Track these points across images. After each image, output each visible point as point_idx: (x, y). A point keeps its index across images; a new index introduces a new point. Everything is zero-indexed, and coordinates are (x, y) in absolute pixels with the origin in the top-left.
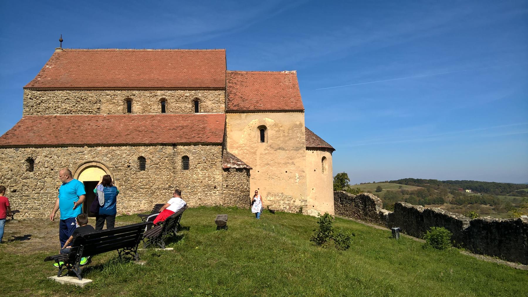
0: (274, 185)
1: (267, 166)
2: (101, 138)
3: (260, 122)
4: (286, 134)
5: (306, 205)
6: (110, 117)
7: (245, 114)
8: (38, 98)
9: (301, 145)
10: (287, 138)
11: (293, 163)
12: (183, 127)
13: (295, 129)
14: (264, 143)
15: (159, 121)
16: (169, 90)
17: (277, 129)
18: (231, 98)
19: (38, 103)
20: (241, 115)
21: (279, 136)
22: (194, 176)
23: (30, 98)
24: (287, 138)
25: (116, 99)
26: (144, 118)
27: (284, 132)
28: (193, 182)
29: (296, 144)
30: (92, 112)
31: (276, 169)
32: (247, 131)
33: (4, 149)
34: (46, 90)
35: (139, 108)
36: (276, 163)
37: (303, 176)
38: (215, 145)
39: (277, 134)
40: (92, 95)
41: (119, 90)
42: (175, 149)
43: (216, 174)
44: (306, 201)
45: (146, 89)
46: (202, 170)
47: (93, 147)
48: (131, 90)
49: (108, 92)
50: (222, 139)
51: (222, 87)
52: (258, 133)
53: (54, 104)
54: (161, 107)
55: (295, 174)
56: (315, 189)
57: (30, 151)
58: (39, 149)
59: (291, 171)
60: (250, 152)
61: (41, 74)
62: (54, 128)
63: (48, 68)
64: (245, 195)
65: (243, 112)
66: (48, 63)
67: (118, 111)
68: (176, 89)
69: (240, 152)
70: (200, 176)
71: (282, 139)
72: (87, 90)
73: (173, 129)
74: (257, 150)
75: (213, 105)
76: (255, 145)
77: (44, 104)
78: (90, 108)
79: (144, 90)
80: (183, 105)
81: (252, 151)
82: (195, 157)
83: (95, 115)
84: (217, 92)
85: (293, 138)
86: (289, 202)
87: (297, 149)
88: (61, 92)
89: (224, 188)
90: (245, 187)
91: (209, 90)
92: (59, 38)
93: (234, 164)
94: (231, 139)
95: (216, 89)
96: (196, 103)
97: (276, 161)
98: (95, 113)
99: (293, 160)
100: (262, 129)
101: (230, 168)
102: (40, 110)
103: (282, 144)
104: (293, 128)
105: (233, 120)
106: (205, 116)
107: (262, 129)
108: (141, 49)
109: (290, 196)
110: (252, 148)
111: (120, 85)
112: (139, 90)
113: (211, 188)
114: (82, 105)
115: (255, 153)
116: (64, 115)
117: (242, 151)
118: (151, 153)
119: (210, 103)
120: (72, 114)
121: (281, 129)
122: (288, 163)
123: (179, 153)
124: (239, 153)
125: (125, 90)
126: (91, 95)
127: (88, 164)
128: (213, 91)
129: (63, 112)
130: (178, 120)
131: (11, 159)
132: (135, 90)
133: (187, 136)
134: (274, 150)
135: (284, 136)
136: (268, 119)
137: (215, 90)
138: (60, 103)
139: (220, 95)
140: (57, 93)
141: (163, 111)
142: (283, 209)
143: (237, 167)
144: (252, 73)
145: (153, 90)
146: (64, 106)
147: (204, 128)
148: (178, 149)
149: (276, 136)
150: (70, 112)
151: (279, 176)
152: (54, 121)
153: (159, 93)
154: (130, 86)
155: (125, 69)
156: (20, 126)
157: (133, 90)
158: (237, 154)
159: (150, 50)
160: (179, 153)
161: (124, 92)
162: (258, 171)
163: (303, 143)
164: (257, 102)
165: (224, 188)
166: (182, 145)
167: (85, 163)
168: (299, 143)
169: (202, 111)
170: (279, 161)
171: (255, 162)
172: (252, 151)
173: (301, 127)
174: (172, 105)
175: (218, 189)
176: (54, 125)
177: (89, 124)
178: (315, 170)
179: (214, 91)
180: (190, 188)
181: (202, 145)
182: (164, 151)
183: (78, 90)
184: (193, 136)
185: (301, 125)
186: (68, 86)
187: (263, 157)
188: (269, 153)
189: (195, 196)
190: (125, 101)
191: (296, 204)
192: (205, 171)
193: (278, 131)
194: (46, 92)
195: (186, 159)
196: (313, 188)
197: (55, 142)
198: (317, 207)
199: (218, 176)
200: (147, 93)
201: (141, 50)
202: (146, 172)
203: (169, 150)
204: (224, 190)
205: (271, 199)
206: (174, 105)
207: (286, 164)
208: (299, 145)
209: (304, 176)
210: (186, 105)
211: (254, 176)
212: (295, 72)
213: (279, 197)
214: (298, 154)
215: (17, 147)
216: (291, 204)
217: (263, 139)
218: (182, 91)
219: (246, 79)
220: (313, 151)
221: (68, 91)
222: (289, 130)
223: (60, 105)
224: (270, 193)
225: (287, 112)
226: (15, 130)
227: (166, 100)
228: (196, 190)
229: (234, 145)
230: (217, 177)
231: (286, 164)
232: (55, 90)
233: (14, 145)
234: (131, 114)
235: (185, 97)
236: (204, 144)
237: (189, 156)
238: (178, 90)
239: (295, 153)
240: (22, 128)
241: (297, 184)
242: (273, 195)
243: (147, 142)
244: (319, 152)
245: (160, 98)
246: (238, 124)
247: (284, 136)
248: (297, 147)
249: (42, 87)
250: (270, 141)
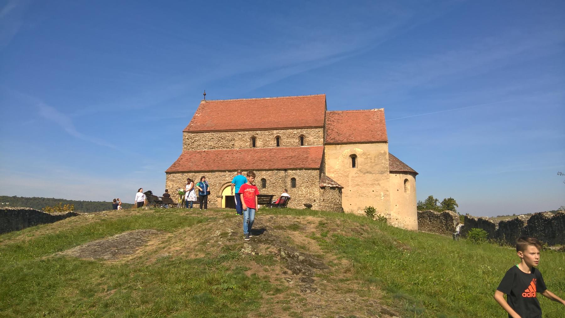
0: (363, 201)
1: (357, 187)
2: (236, 166)
3: (351, 152)
6: (241, 151)
7: (340, 145)
8: (192, 138)
10: (373, 164)
11: (378, 184)
12: (292, 157)
13: (380, 156)
14: (354, 169)
15: (275, 153)
16: (282, 130)
17: (365, 157)
18: (329, 133)
19: (192, 142)
20: (336, 147)
21: (367, 162)
22: (300, 192)
23: (187, 139)
24: (373, 164)
25: (245, 137)
26: (265, 151)
27: (371, 160)
28: (299, 197)
29: (381, 168)
30: (229, 147)
32: (341, 159)
33: (175, 174)
34: (197, 133)
35: (261, 144)
36: (364, 184)
37: (387, 195)
38: (315, 170)
39: (365, 161)
40: (229, 135)
41: (247, 131)
42: (286, 173)
43: (315, 191)
44: (390, 215)
45: (266, 129)
46: (305, 188)
47: (232, 172)
48: (255, 131)
49: (240, 133)
50: (319, 165)
51: (321, 125)
52: (350, 160)
53: (203, 142)
54: (276, 142)
55: (381, 193)
56: (398, 205)
57: (191, 175)
58: (197, 174)
59: (377, 191)
60: (343, 175)
61: (193, 121)
62: (205, 159)
63: (197, 116)
64: (338, 207)
65: (338, 144)
66: (196, 112)
67: (246, 146)
68: (287, 128)
69: (336, 176)
70: (304, 192)
71: (369, 165)
72: (226, 132)
73: (285, 158)
74: (349, 174)
75: (314, 139)
76: (348, 170)
77: (196, 143)
78: (227, 145)
79: (265, 130)
80: (292, 140)
81: (345, 174)
82: (300, 179)
83: (230, 150)
84: (317, 130)
85: (379, 164)
87: (382, 173)
88: (208, 133)
89: (321, 201)
90: (338, 201)
91: (311, 128)
92: (204, 93)
93: (329, 183)
94: (328, 165)
95: (317, 127)
96: (302, 138)
97: (365, 183)
98: (230, 148)
99: (378, 182)
100: (354, 157)
101: (326, 187)
102: (194, 147)
103: (370, 169)
104: (378, 156)
105: (329, 150)
106: (308, 148)
107: (354, 157)
108: (262, 98)
110: (345, 172)
111: (248, 128)
112: (261, 130)
113: (312, 201)
114: (222, 142)
115: (347, 176)
116: (210, 150)
117: (337, 175)
118: (270, 176)
119: (312, 138)
120: (215, 149)
121: (369, 156)
122: (375, 184)
123: (289, 176)
125: (251, 131)
126: (228, 135)
127: (228, 184)
128: (314, 129)
129: (209, 148)
130: (288, 152)
131: (179, 181)
132: (258, 130)
133: (294, 164)
134: (363, 173)
135: (371, 162)
136: (358, 149)
137: (316, 128)
138: (207, 141)
139: (319, 132)
140: (205, 134)
141: (278, 145)
143: (331, 186)
144: (347, 112)
145: (271, 130)
146: (210, 143)
147: (307, 157)
148: (289, 173)
149: (365, 163)
150: (214, 147)
151: (367, 194)
152: (204, 154)
153: (275, 132)
154: (255, 128)
155: (251, 115)
156: (182, 159)
157: (257, 130)
158: (333, 177)
159: (268, 98)
160: (289, 176)
161: (251, 132)
162: (350, 191)
163: (387, 168)
164: (350, 136)
165: (321, 201)
166: (291, 170)
167: (226, 183)
168: (384, 168)
169: (306, 144)
170: (367, 182)
171: (348, 183)
172: (345, 174)
173: (386, 155)
174: (284, 141)
175: (317, 202)
176: (204, 157)
177: (228, 156)
178: (398, 190)
179: (315, 129)
180: (296, 201)
181: (305, 170)
182: (279, 174)
183: (219, 132)
184: (299, 163)
185: (385, 153)
186: (212, 129)
187: (354, 180)
188: (359, 176)
189: (300, 207)
190: (251, 139)
192: (307, 189)
193: (366, 158)
194: (197, 134)
195: (293, 180)
197: (208, 169)
199: (317, 192)
200: (267, 133)
201: (262, 99)
202: (266, 189)
203: (282, 173)
204: (321, 203)
206: (285, 140)
207: (372, 184)
209: (388, 194)
210: (294, 140)
211: (348, 195)
212: (382, 109)
214: (383, 177)
215: (183, 172)
217: (354, 165)
218: (292, 130)
219: (342, 117)
220: (396, 174)
221: (213, 133)
222: (375, 157)
223: (207, 143)
224: (360, 208)
225: (374, 143)
226: (180, 161)
227: (280, 137)
228: (301, 203)
229: (331, 170)
230: (316, 193)
231: (372, 184)
232: (204, 132)
233: (181, 171)
234: (255, 148)
235: (294, 134)
236: (306, 169)
237: (296, 178)
238: (288, 129)
239: (381, 175)
240: (184, 159)
241: (382, 201)
243: (267, 168)
244: (401, 175)
245: (276, 135)
246: (334, 153)
247: (371, 162)
248: (382, 171)
249: (195, 130)
250: (360, 167)
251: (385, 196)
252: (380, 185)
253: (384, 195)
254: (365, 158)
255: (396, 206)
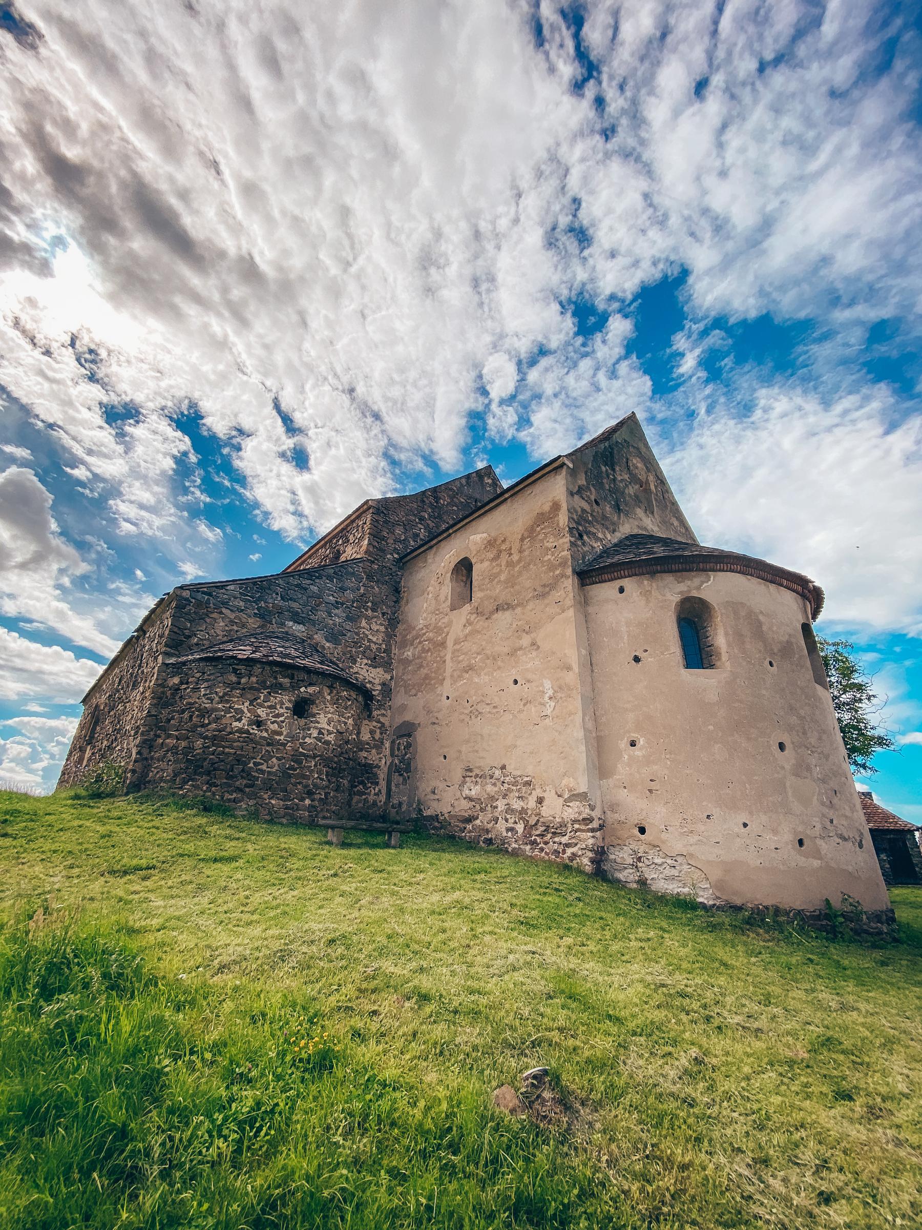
4: (515, 557)
5: (584, 819)
9: (557, 572)
13: (538, 529)
31: (487, 678)
55: (542, 685)
56: (641, 742)
86: (522, 803)
97: (489, 652)
109: (526, 779)
122: (520, 649)
124: (414, 655)
142: (505, 834)
178: (637, 659)
188: (475, 632)
191: (546, 811)
196: (634, 736)
198: (664, 836)
205: (473, 792)
207: (513, 653)
208: (551, 574)
213: (494, 785)
214: (547, 609)
216: (530, 812)
222: (522, 539)
224: (470, 770)
231: (513, 653)
242: (477, 776)
247: (510, 564)
248: (544, 586)
251: (559, 695)
252: (538, 647)
253: (555, 692)
254: (492, 556)
255: (633, 744)
